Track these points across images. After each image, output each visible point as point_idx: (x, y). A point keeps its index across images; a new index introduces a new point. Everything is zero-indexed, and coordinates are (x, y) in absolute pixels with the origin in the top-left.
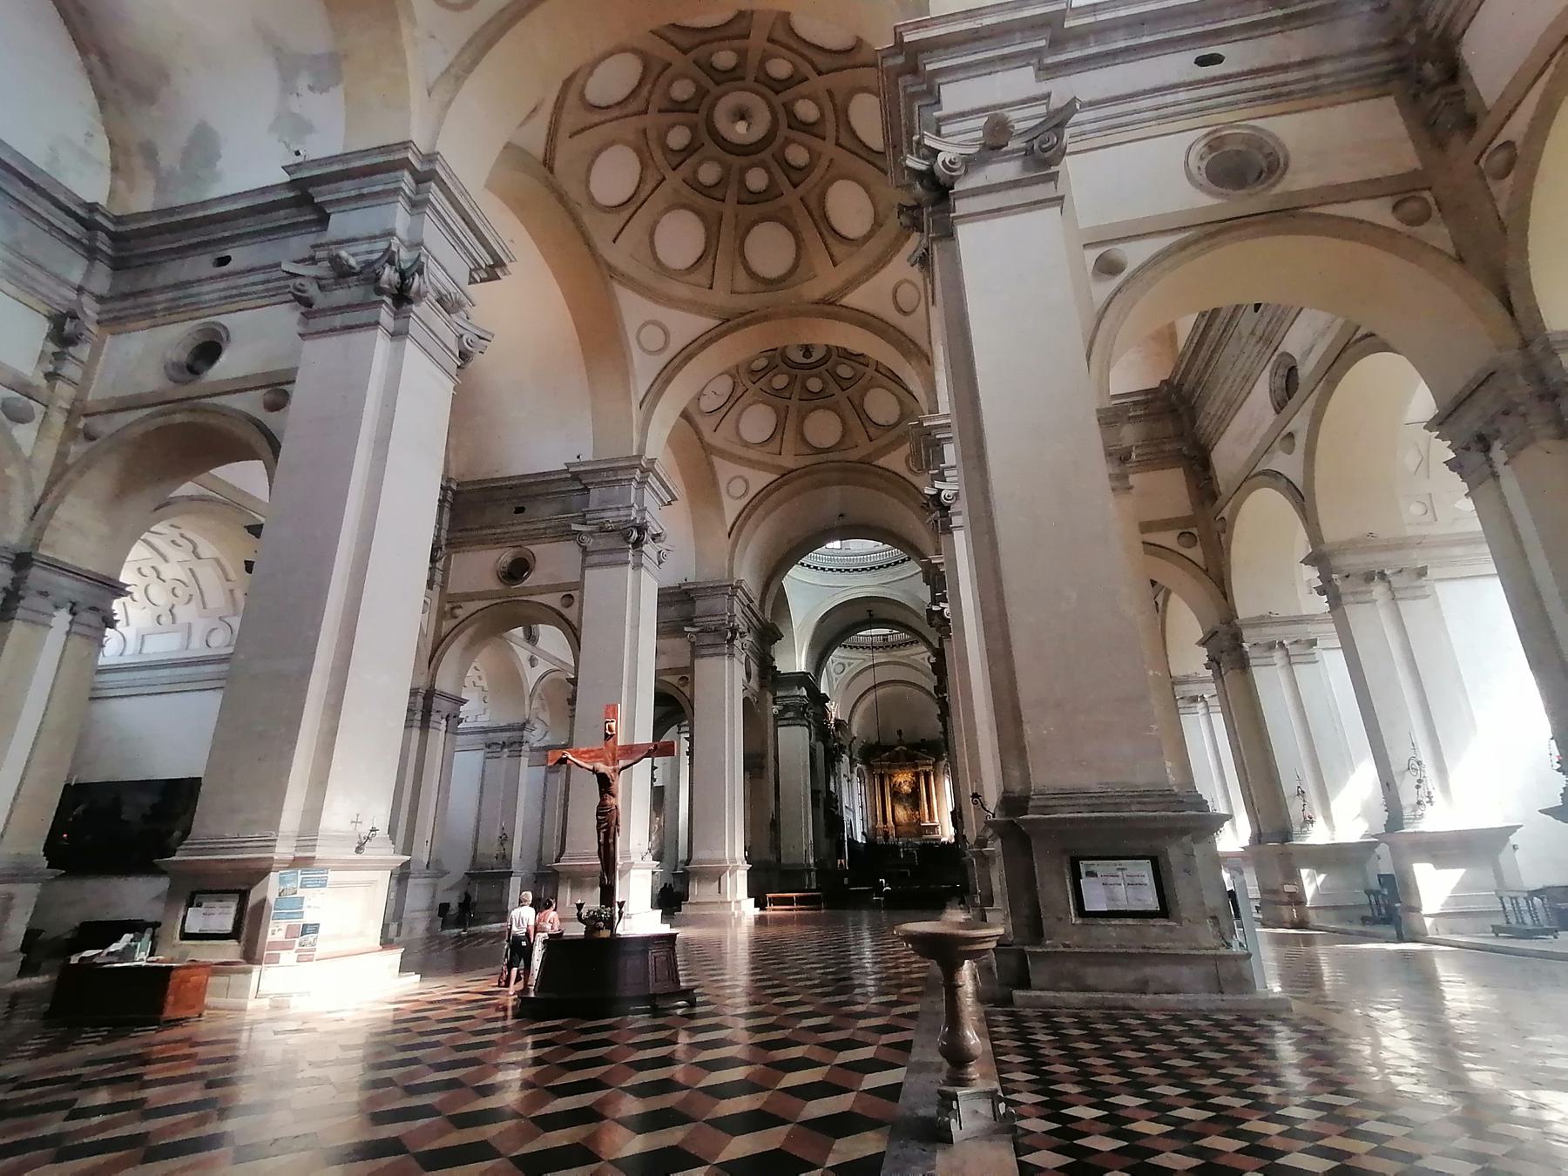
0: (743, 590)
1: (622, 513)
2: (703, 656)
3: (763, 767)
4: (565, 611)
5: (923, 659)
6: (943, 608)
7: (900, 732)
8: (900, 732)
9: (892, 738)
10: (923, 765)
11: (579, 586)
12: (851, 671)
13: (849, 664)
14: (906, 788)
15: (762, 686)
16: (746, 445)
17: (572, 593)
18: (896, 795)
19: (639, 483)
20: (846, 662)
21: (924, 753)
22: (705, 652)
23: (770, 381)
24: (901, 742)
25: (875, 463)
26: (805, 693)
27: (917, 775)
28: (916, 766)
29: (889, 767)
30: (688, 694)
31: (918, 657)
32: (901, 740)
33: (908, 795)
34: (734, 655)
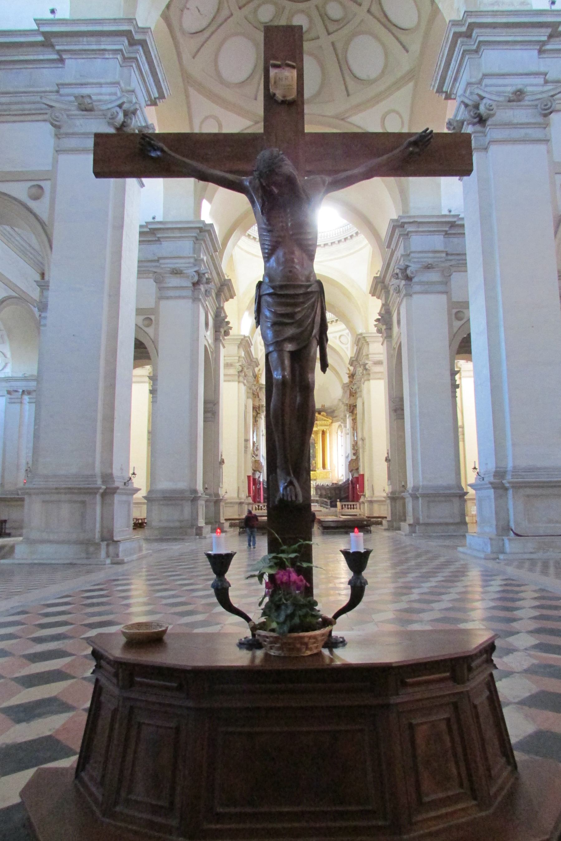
0: (210, 235)
1: (104, 90)
2: (168, 298)
3: (215, 413)
4: (32, 204)
5: (335, 337)
6: (407, 267)
10: (321, 425)
11: (50, 176)
15: (217, 339)
16: (223, 82)
17: (42, 183)
19: (124, 58)
21: (323, 416)
22: (171, 293)
23: (256, 10)
25: (349, 120)
26: (243, 355)
30: (152, 335)
34: (200, 300)
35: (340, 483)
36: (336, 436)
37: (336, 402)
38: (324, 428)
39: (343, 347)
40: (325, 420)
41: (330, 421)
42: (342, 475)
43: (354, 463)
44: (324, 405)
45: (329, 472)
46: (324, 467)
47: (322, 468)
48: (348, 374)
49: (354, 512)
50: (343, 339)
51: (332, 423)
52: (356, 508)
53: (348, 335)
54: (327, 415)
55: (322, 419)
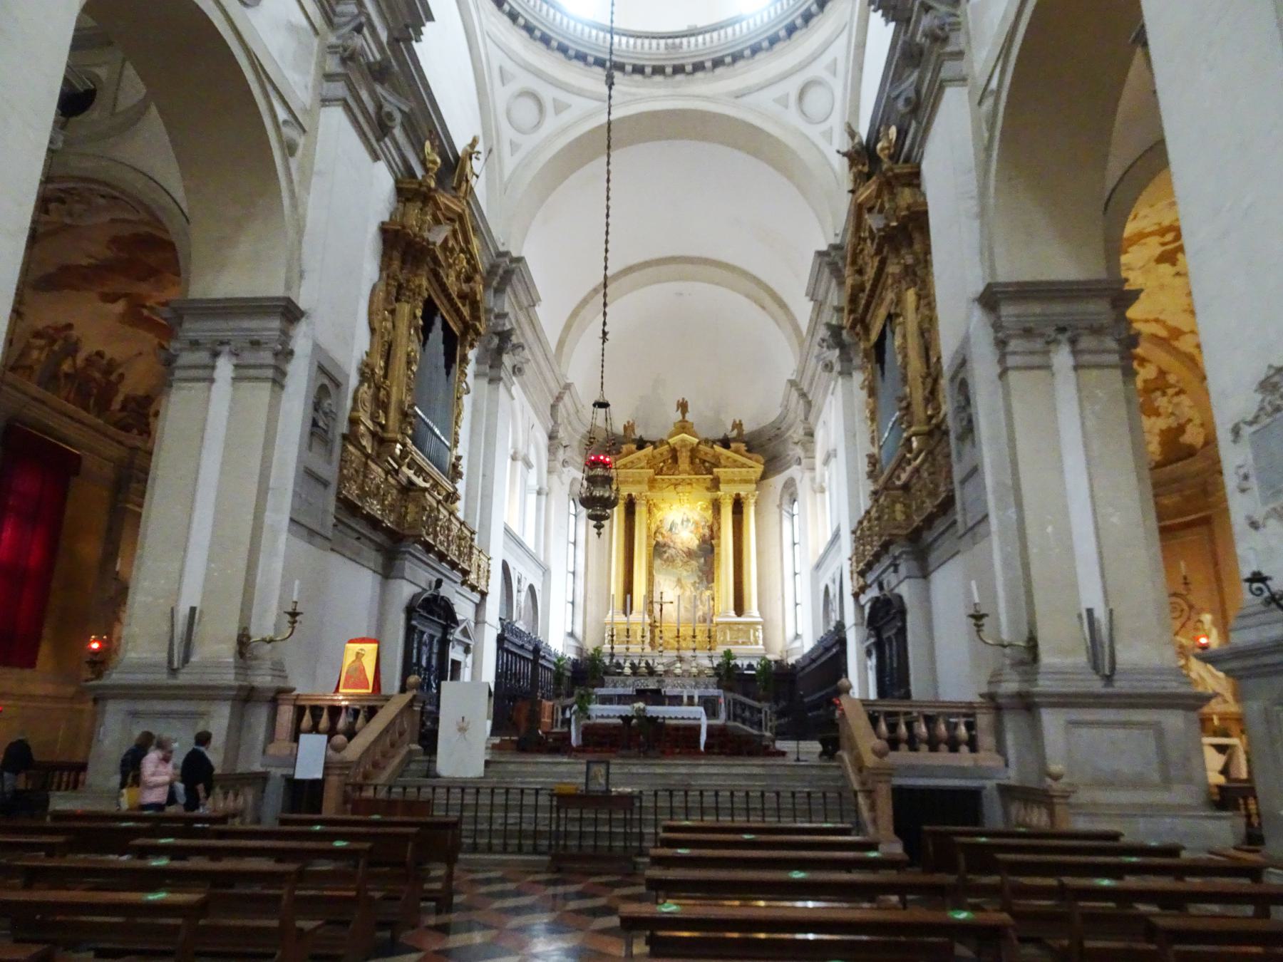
7: (683, 406)
8: (683, 406)
9: (660, 424)
12: (564, 130)
13: (559, 108)
14: (687, 538)
18: (658, 549)
20: (547, 93)
21: (737, 452)
24: (683, 427)
27: (716, 506)
28: (716, 484)
29: (652, 483)
31: (766, 98)
32: (684, 420)
33: (690, 554)
35: (791, 661)
36: (777, 517)
37: (773, 415)
38: (743, 490)
39: (814, 132)
40: (743, 466)
41: (760, 469)
42: (797, 636)
43: (899, 507)
44: (741, 424)
45: (757, 623)
46: (739, 608)
47: (732, 613)
48: (845, 155)
49: (962, 772)
50: (816, 101)
51: (764, 476)
52: (973, 745)
53: (834, 73)
54: (748, 451)
55: (735, 461)
